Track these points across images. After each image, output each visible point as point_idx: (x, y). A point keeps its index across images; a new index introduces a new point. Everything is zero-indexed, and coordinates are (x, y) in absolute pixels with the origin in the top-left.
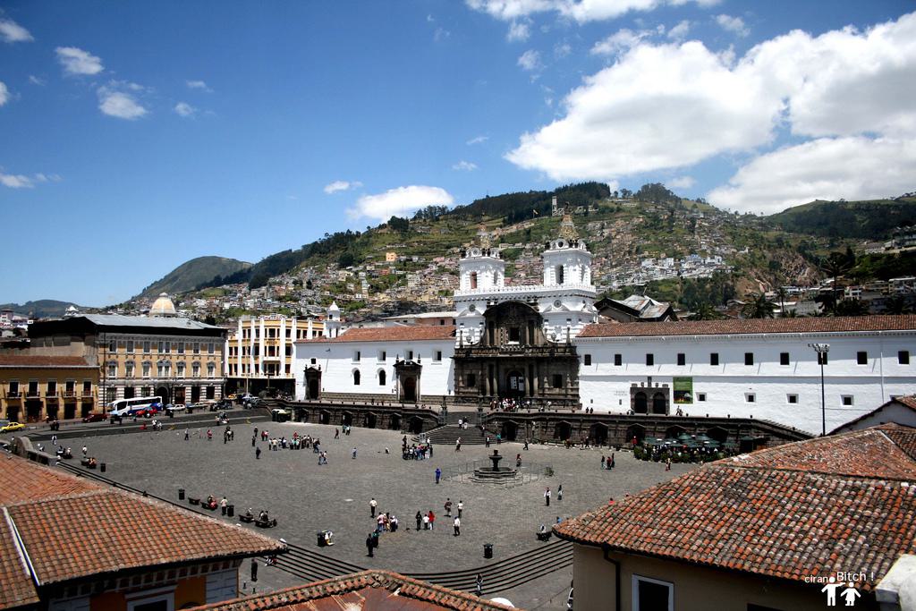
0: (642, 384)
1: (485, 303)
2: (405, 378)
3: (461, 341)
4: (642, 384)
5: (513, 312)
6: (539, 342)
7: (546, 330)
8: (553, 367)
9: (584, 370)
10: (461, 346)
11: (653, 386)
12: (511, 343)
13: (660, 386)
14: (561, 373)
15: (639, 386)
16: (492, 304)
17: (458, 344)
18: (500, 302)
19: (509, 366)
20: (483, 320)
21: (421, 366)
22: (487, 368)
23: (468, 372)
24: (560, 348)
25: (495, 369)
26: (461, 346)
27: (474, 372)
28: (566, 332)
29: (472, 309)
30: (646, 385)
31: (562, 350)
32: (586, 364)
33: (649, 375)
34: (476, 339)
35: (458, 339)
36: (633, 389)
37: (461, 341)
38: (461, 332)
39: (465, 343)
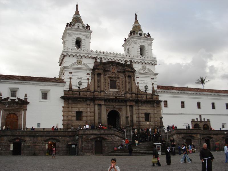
0: (197, 119)
1: (94, 61)
2: (7, 113)
3: (70, 85)
4: (197, 119)
5: (114, 69)
6: (135, 90)
7: (138, 83)
8: (144, 108)
9: (164, 110)
10: (70, 88)
11: (203, 120)
12: (111, 90)
13: (206, 120)
14: (149, 112)
15: (196, 120)
16: (98, 60)
17: (68, 87)
18: (104, 61)
19: (110, 107)
20: (90, 72)
21: (29, 103)
22: (96, 106)
23: (77, 110)
24: (148, 95)
25: (103, 107)
26: (70, 88)
27: (81, 110)
28: (152, 86)
29: (79, 62)
30: (199, 120)
31: (150, 96)
32: (165, 107)
33: (200, 113)
34: (84, 85)
35: (68, 83)
36: (193, 121)
37: (70, 85)
38: (70, 78)
39: (75, 87)
